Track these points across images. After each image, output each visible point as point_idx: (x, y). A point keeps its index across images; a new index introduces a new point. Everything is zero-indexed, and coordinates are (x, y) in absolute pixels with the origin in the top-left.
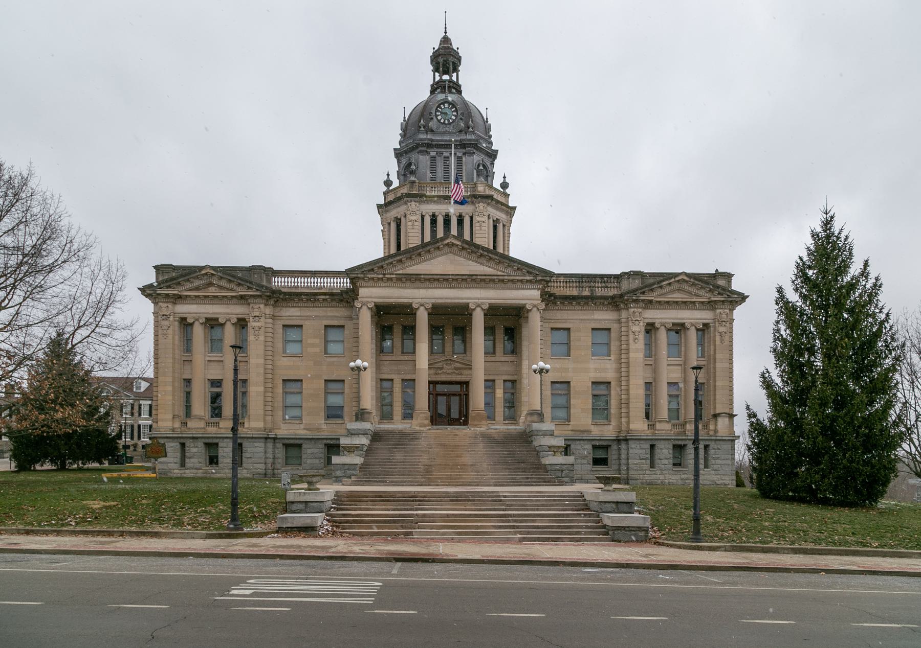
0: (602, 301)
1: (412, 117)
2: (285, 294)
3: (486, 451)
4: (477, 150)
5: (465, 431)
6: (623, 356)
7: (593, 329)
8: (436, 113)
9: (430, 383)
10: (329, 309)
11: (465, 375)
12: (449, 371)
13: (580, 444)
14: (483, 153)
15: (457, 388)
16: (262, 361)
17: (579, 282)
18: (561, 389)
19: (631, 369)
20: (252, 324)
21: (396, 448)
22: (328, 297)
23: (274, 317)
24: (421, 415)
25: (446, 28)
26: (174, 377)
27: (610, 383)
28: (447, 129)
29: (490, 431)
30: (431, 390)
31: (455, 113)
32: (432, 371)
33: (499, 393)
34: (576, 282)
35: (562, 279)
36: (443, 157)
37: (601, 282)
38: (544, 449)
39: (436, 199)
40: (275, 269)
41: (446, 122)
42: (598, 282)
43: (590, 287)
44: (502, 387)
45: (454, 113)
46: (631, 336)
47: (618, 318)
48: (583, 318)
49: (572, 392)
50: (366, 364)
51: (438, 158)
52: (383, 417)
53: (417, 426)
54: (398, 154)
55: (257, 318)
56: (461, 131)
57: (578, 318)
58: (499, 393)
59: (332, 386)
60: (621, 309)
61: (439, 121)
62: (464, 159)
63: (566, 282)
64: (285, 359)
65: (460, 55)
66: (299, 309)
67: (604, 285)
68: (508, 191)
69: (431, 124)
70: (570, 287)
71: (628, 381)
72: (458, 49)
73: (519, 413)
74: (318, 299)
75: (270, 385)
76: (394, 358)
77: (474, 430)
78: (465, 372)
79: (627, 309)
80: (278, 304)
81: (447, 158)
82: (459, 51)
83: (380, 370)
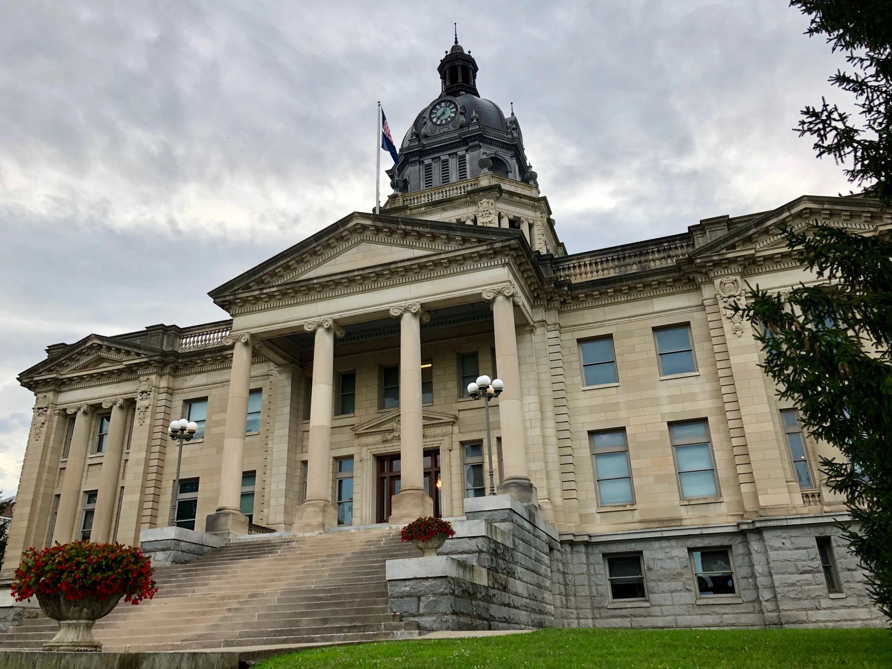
0: (660, 277)
4: (483, 142)
7: (655, 329)
8: (430, 116)
11: (431, 437)
13: (661, 548)
14: (495, 145)
16: (143, 455)
17: (619, 259)
20: (140, 404)
23: (171, 391)
25: (456, 35)
26: (36, 494)
27: (705, 420)
31: (455, 110)
35: (587, 260)
37: (659, 251)
39: (423, 209)
45: (452, 110)
55: (144, 394)
56: (462, 127)
62: (468, 156)
63: (596, 263)
65: (473, 57)
66: (205, 374)
67: (665, 255)
70: (603, 270)
72: (469, 52)
79: (711, 281)
82: (471, 54)
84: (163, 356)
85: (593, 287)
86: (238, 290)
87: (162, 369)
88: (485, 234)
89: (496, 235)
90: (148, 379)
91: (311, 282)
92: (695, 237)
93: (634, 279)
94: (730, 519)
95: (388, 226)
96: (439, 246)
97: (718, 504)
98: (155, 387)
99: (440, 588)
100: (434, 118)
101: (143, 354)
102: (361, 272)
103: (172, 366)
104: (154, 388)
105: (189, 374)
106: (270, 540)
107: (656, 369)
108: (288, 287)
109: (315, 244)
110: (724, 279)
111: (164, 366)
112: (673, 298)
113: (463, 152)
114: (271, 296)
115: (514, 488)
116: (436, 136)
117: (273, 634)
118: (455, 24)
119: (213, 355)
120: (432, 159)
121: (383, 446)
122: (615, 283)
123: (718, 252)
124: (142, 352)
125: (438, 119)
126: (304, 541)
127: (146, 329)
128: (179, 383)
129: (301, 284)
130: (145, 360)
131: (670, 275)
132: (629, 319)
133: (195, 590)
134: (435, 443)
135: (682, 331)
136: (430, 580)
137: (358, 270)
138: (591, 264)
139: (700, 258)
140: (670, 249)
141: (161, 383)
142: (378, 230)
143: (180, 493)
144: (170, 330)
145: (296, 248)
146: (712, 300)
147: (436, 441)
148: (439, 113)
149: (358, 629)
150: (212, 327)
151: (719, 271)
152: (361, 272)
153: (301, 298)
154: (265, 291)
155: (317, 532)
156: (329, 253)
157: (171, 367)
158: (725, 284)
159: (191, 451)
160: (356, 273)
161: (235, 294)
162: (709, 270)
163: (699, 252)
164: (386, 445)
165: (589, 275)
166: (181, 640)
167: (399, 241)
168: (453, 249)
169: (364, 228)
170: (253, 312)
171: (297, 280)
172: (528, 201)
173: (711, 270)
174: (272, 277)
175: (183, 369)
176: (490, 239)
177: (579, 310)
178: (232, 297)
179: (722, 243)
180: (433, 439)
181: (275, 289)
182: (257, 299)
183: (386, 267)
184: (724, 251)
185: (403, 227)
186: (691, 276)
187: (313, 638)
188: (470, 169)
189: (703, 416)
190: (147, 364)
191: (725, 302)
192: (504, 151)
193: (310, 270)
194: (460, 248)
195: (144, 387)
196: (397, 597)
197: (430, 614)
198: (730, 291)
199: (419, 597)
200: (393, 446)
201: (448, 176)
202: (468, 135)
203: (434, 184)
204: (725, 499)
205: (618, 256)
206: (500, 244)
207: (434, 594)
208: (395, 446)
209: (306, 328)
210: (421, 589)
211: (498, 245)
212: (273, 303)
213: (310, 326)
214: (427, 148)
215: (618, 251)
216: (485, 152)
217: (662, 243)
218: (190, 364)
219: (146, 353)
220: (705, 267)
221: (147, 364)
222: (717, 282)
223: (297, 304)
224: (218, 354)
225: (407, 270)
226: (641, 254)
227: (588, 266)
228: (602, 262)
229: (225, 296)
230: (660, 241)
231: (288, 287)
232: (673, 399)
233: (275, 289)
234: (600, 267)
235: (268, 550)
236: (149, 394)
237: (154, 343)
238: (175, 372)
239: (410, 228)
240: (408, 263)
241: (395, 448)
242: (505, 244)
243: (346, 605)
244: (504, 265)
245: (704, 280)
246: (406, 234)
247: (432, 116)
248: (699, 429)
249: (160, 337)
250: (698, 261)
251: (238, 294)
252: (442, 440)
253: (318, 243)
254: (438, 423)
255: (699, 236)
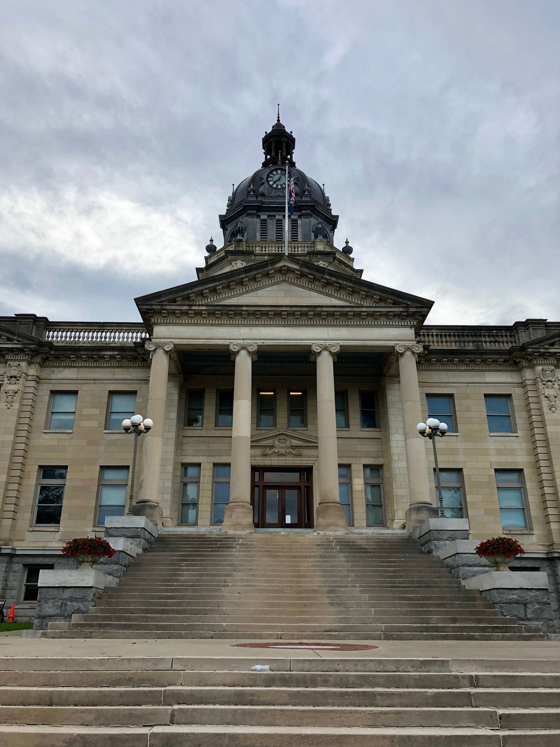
0: (495, 357)
1: (240, 187)
2: (58, 348)
3: (351, 566)
5: (308, 536)
6: (536, 431)
7: (486, 396)
9: (254, 469)
10: (117, 370)
11: (306, 456)
12: (283, 451)
14: (321, 218)
15: (293, 478)
17: (459, 336)
18: (449, 479)
19: (552, 447)
21: (185, 560)
22: (116, 353)
23: (38, 380)
24: (237, 510)
25: (278, 114)
27: (520, 471)
28: (280, 193)
29: (350, 536)
30: (257, 479)
32: (258, 451)
33: (358, 483)
34: (454, 336)
36: (275, 220)
37: (489, 336)
38: (465, 561)
40: (50, 320)
41: (279, 187)
42: (485, 336)
43: (474, 342)
44: (362, 475)
46: (545, 403)
47: (520, 381)
48: (470, 380)
49: (466, 483)
50: (149, 422)
51: (269, 221)
52: (182, 522)
53: (230, 528)
54: (224, 221)
55: (13, 379)
57: (463, 381)
58: (358, 483)
59: (110, 476)
60: (523, 368)
61: (271, 186)
62: (299, 222)
63: (441, 336)
64: (46, 436)
65: (294, 137)
67: (492, 339)
68: (351, 256)
69: (261, 189)
70: (446, 342)
71: (551, 466)
72: (291, 132)
73: (389, 515)
74: (103, 357)
75: (18, 473)
76: (203, 433)
77: (324, 535)
78: (305, 452)
79: (533, 367)
80: (48, 363)
81: (280, 224)
83: (183, 450)
84: (38, 346)
85: (444, 354)
86: (165, 301)
87: (32, 357)
88: (402, 298)
89: (412, 301)
90: (19, 365)
91: (240, 308)
92: (519, 331)
93: (476, 354)
94: (540, 547)
95: (314, 274)
96: (356, 300)
97: (530, 536)
98: (25, 374)
99: (543, 598)
100: (271, 181)
101: (16, 340)
102: (288, 309)
103: (44, 356)
104: (24, 375)
105: (58, 367)
106: (205, 535)
107: (487, 426)
108: (218, 308)
109: (244, 276)
110: (546, 367)
111: (36, 355)
112: (500, 373)
113: (296, 217)
114: (198, 313)
115: (426, 511)
116: (272, 197)
117: (419, 630)
118: (279, 105)
119: (89, 353)
120: (269, 216)
121: (262, 459)
122: (462, 354)
123: (543, 346)
124: (16, 338)
125: (274, 182)
126: (342, 545)
127: (15, 316)
128: (46, 373)
129: (230, 308)
130: (19, 346)
131: (503, 357)
132: (467, 384)
133: (226, 581)
134: (309, 462)
135: (503, 400)
136: (533, 591)
137: (286, 306)
138: (437, 335)
139: (532, 348)
140: (497, 336)
141: (29, 370)
142: (302, 275)
143: (42, 478)
144: (40, 321)
145: (226, 275)
146: (532, 381)
147: (310, 461)
148: (276, 178)
149: (501, 629)
150: (84, 326)
151: (540, 361)
152: (288, 309)
153: (225, 320)
154: (194, 308)
155: (248, 531)
156: (254, 285)
157: (42, 357)
158: (546, 371)
159: (58, 440)
160: (284, 309)
161: (163, 305)
162: (534, 358)
163: (532, 344)
164: (264, 459)
165: (436, 344)
166: (324, 630)
167: (318, 288)
168: (367, 305)
169: (289, 270)
170: (175, 324)
171: (219, 303)
172: (350, 271)
173: (535, 358)
174: (197, 296)
175: (52, 361)
176: (405, 304)
177: (428, 370)
178: (159, 307)
179: (547, 340)
180: (307, 459)
181: (204, 308)
182: (185, 313)
183: (312, 309)
184: (547, 346)
185: (328, 277)
186: (517, 361)
187: (472, 636)
188: (302, 232)
189: (520, 467)
190: (21, 351)
191: (544, 384)
192: (326, 224)
193: (232, 297)
194: (374, 305)
195: (14, 372)
196: (506, 603)
197: (537, 619)
198: (549, 377)
199: (525, 605)
200: (271, 460)
201: (282, 233)
202: (303, 204)
203: (269, 238)
204: (535, 532)
205: (459, 333)
206: (414, 310)
207: (538, 603)
208: (288, 460)
209: (232, 348)
210: (528, 598)
211: (412, 310)
212: (197, 320)
213: (235, 347)
214: (265, 206)
215: (459, 330)
216: (313, 221)
217: (492, 330)
218: (62, 358)
219: (19, 339)
220: (531, 355)
221: (21, 351)
222: (539, 368)
223: (220, 325)
224: (95, 353)
225: (331, 315)
226: (476, 336)
227: (435, 336)
228: (445, 336)
229: (152, 305)
230: (491, 328)
231: (218, 308)
232: (499, 452)
233: (204, 308)
234: (444, 339)
235: (220, 544)
236: (19, 380)
237: (22, 329)
238: (45, 363)
239: (335, 279)
240: (333, 309)
241: (272, 462)
242: (418, 310)
243: (447, 606)
244: (411, 327)
245: (527, 365)
246: (328, 284)
247: (269, 179)
248: (515, 476)
249: (31, 326)
250: (530, 350)
251: (165, 305)
252: (316, 461)
253: (248, 274)
254: (314, 446)
255: (522, 330)
